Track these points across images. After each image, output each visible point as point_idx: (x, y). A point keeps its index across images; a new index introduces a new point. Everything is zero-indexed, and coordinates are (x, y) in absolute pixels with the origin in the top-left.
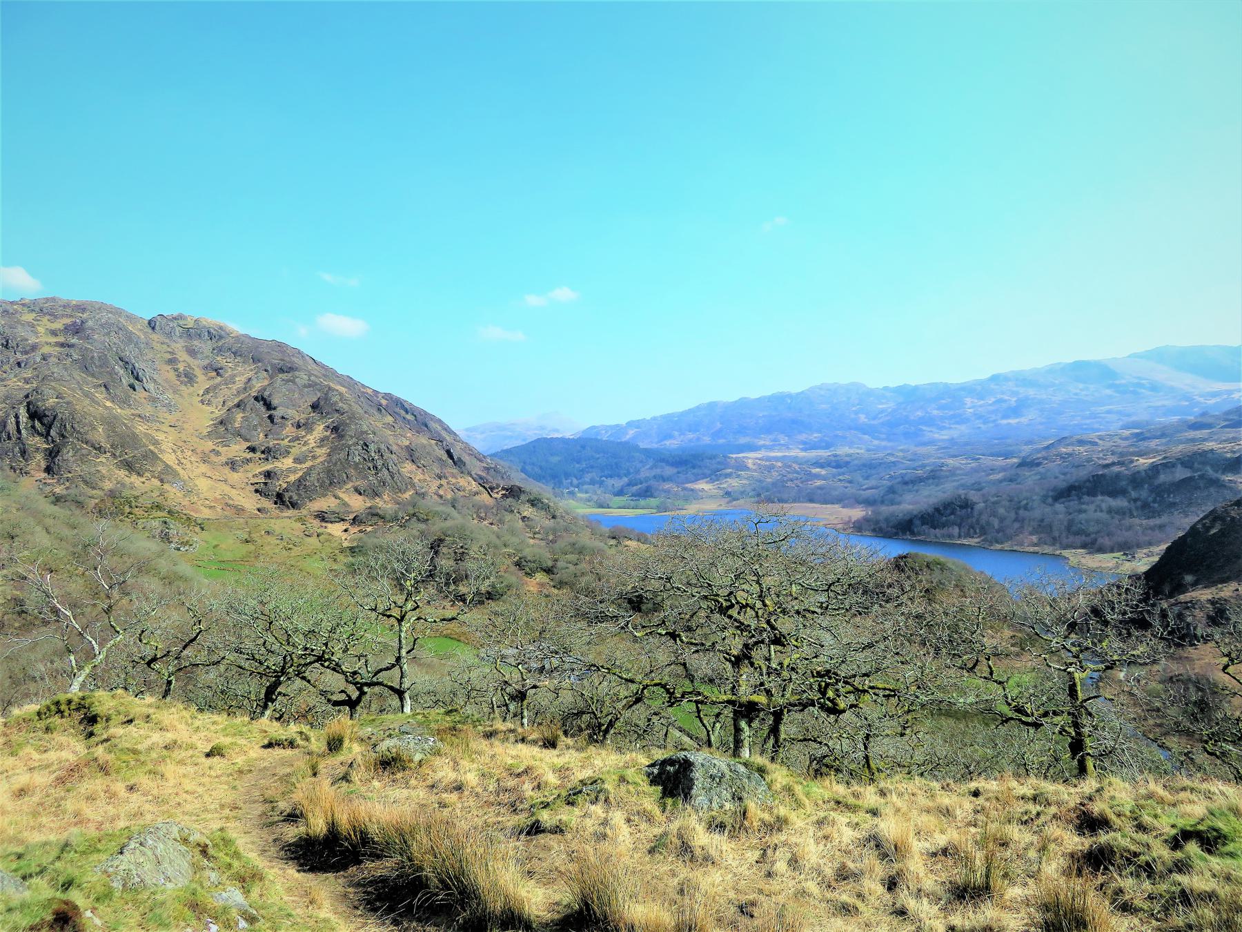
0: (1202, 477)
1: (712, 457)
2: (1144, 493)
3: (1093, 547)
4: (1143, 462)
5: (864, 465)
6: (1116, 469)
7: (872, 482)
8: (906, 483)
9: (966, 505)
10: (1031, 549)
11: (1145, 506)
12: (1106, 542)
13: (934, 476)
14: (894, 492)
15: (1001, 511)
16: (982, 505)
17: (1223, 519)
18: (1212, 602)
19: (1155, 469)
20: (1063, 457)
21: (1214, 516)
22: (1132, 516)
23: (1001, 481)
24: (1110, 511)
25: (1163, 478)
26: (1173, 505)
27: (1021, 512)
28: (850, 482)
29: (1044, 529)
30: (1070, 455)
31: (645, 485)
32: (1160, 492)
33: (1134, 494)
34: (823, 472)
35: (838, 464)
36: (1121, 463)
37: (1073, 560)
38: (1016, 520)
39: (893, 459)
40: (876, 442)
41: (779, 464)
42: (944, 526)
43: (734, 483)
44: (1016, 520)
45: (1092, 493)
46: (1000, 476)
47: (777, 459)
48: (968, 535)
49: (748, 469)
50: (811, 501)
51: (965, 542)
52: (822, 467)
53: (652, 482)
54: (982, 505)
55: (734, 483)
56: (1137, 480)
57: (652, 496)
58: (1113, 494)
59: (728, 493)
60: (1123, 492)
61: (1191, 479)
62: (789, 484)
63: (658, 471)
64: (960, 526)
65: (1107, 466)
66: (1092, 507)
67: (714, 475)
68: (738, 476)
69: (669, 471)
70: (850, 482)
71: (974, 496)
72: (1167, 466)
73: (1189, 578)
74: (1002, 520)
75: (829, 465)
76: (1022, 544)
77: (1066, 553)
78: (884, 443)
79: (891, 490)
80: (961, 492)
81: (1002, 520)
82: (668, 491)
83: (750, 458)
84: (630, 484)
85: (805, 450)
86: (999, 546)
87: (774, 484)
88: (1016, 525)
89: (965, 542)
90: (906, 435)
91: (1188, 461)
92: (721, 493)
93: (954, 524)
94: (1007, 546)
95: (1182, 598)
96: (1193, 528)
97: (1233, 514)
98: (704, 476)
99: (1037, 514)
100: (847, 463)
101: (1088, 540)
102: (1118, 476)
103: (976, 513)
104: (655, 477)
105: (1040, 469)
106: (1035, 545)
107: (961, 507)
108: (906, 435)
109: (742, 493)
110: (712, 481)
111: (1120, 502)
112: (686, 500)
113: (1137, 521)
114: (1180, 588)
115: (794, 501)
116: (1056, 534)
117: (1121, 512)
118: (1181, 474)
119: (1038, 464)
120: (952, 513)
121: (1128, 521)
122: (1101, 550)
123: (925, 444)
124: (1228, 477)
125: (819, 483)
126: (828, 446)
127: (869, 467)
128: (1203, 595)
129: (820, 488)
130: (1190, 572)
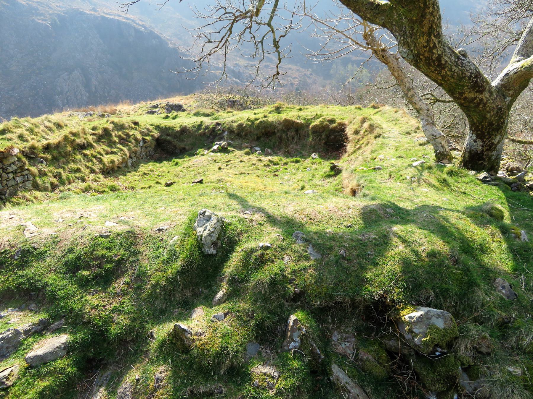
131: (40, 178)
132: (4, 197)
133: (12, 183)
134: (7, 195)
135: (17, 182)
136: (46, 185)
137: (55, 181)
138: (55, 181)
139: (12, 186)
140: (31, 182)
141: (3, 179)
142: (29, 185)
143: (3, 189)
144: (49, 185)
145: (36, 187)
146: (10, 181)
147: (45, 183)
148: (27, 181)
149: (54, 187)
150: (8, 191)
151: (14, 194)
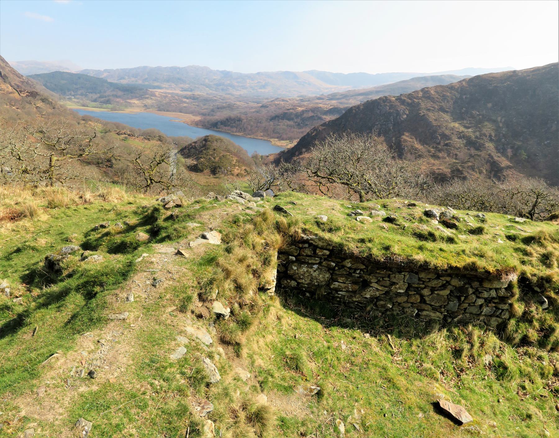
0: (316, 116)
1: (140, 89)
2: (299, 120)
3: (281, 138)
4: (300, 109)
5: (204, 100)
6: (291, 111)
7: (206, 107)
8: (218, 108)
9: (240, 120)
10: (260, 138)
11: (299, 125)
12: (285, 136)
13: (230, 107)
14: (213, 112)
15: (252, 123)
16: (245, 120)
17: (316, 130)
18: (308, 158)
19: (303, 112)
20: (276, 105)
21: (315, 129)
22: (294, 128)
23: (254, 112)
24: (287, 126)
25: (305, 115)
26: (307, 125)
27: (259, 124)
28: (198, 106)
29: (265, 130)
30: (278, 104)
31: (107, 98)
32: (303, 120)
33: (296, 120)
34: (187, 101)
35: (194, 98)
36: (293, 109)
37: (273, 143)
38: (257, 127)
39: (215, 98)
40: (211, 91)
41: (170, 96)
42: (232, 127)
43: (149, 102)
44: (257, 127)
45: (283, 119)
46: (254, 110)
47: (169, 93)
48: (239, 132)
49: (156, 96)
50: (181, 112)
51: (238, 134)
52: (187, 98)
53: (111, 98)
54: (245, 120)
55: (149, 102)
56: (297, 115)
57: (110, 104)
58: (289, 119)
59: (145, 106)
60: (292, 119)
61: (313, 116)
62: (172, 104)
63: (115, 93)
64: (236, 128)
65: (289, 109)
66: (282, 124)
67: (140, 98)
68: (151, 99)
69: (120, 93)
70: (198, 106)
71: (243, 117)
72: (306, 111)
73: (304, 150)
74: (252, 126)
75: (190, 98)
76: (257, 136)
77: (272, 140)
78: (214, 92)
79: (213, 111)
80: (238, 115)
81: (252, 126)
82: (118, 102)
83: (158, 92)
84: (100, 97)
85: (182, 91)
86: (249, 136)
87: (166, 104)
88: (256, 129)
89: (238, 134)
90: (222, 90)
91: (313, 110)
92: (143, 105)
93: (235, 127)
94: (252, 136)
95: (301, 156)
96: (308, 133)
97: (320, 129)
98: (136, 97)
99: (264, 125)
100: (198, 98)
101: (279, 136)
102: (291, 113)
103: (243, 123)
104: (113, 95)
105: (268, 109)
106: (262, 136)
107: (238, 121)
108: (222, 90)
109: (152, 106)
110: (139, 100)
111: (291, 123)
112: (126, 107)
113: (295, 130)
114: (301, 153)
115: (174, 111)
116: (269, 133)
117: (291, 126)
118: (311, 114)
119: (267, 107)
120: (235, 123)
121: (293, 129)
122: (283, 139)
123: (229, 94)
124: (324, 117)
125: (185, 105)
126: (191, 91)
127: (206, 100)
128: (306, 155)
129: (185, 107)
130: (304, 147)
131: (518, 322)
132: (449, 320)
133: (474, 310)
134: (456, 320)
135: (482, 312)
136: (515, 335)
137: (534, 335)
138: (534, 335)
139: (471, 313)
140: (500, 320)
141: (466, 301)
142: (494, 322)
143: (457, 312)
144: (518, 337)
145: (501, 330)
146: (473, 308)
147: (517, 331)
148: (497, 316)
149: (525, 341)
150: (460, 317)
151: (464, 323)
